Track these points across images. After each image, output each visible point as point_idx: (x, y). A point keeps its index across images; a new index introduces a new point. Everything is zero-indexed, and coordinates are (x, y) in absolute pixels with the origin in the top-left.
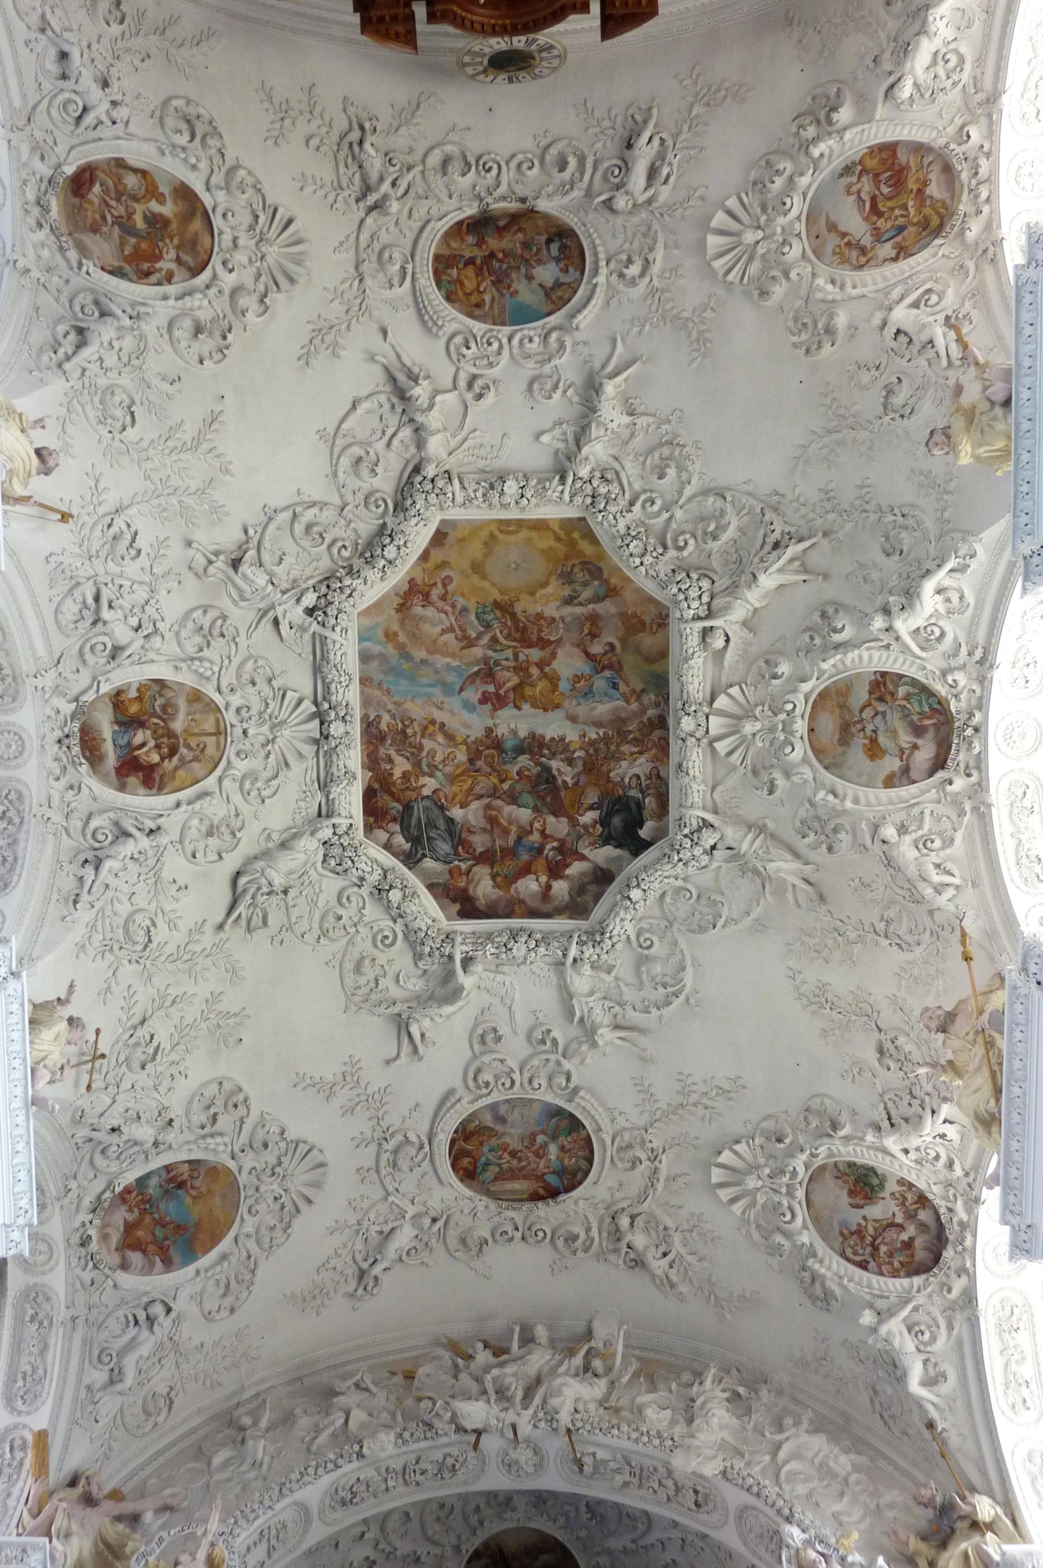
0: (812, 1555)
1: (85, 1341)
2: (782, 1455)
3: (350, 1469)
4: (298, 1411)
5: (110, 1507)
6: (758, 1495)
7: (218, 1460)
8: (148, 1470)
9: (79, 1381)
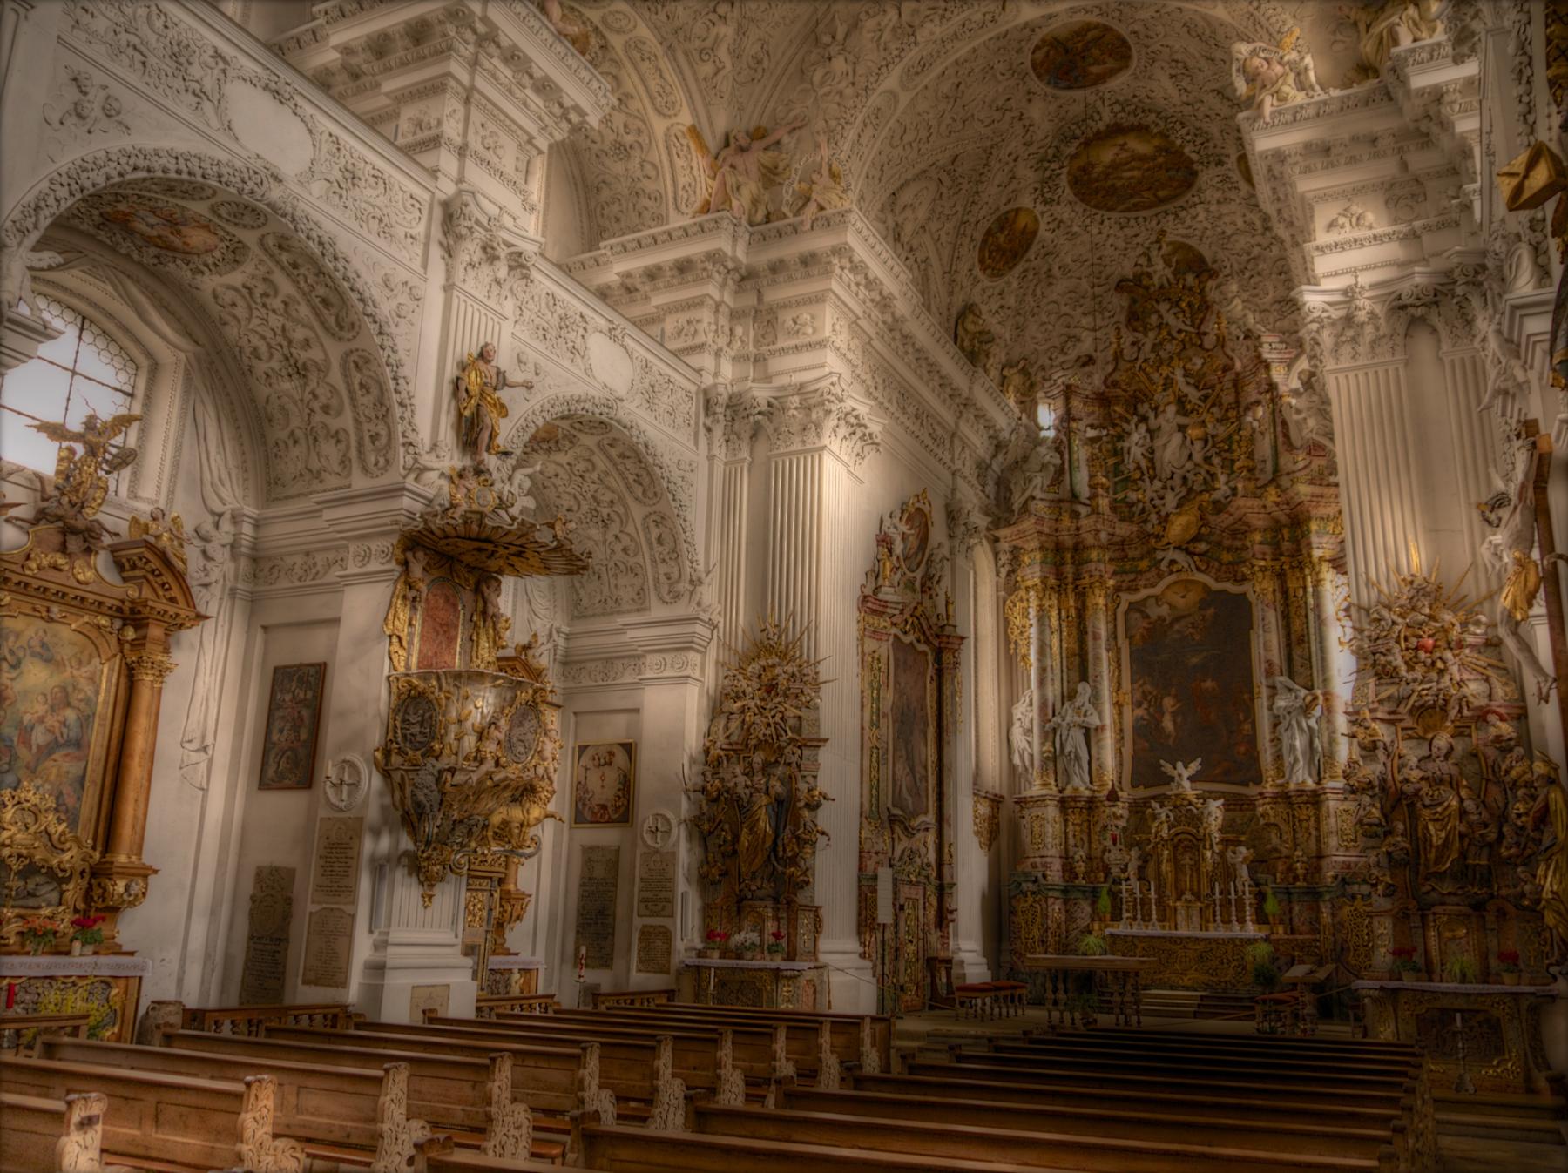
0: (1256, 62)
1: (686, 53)
3: (912, 55)
4: (863, 16)
5: (757, 145)
7: (817, 78)
8: (773, 100)
9: (697, 80)
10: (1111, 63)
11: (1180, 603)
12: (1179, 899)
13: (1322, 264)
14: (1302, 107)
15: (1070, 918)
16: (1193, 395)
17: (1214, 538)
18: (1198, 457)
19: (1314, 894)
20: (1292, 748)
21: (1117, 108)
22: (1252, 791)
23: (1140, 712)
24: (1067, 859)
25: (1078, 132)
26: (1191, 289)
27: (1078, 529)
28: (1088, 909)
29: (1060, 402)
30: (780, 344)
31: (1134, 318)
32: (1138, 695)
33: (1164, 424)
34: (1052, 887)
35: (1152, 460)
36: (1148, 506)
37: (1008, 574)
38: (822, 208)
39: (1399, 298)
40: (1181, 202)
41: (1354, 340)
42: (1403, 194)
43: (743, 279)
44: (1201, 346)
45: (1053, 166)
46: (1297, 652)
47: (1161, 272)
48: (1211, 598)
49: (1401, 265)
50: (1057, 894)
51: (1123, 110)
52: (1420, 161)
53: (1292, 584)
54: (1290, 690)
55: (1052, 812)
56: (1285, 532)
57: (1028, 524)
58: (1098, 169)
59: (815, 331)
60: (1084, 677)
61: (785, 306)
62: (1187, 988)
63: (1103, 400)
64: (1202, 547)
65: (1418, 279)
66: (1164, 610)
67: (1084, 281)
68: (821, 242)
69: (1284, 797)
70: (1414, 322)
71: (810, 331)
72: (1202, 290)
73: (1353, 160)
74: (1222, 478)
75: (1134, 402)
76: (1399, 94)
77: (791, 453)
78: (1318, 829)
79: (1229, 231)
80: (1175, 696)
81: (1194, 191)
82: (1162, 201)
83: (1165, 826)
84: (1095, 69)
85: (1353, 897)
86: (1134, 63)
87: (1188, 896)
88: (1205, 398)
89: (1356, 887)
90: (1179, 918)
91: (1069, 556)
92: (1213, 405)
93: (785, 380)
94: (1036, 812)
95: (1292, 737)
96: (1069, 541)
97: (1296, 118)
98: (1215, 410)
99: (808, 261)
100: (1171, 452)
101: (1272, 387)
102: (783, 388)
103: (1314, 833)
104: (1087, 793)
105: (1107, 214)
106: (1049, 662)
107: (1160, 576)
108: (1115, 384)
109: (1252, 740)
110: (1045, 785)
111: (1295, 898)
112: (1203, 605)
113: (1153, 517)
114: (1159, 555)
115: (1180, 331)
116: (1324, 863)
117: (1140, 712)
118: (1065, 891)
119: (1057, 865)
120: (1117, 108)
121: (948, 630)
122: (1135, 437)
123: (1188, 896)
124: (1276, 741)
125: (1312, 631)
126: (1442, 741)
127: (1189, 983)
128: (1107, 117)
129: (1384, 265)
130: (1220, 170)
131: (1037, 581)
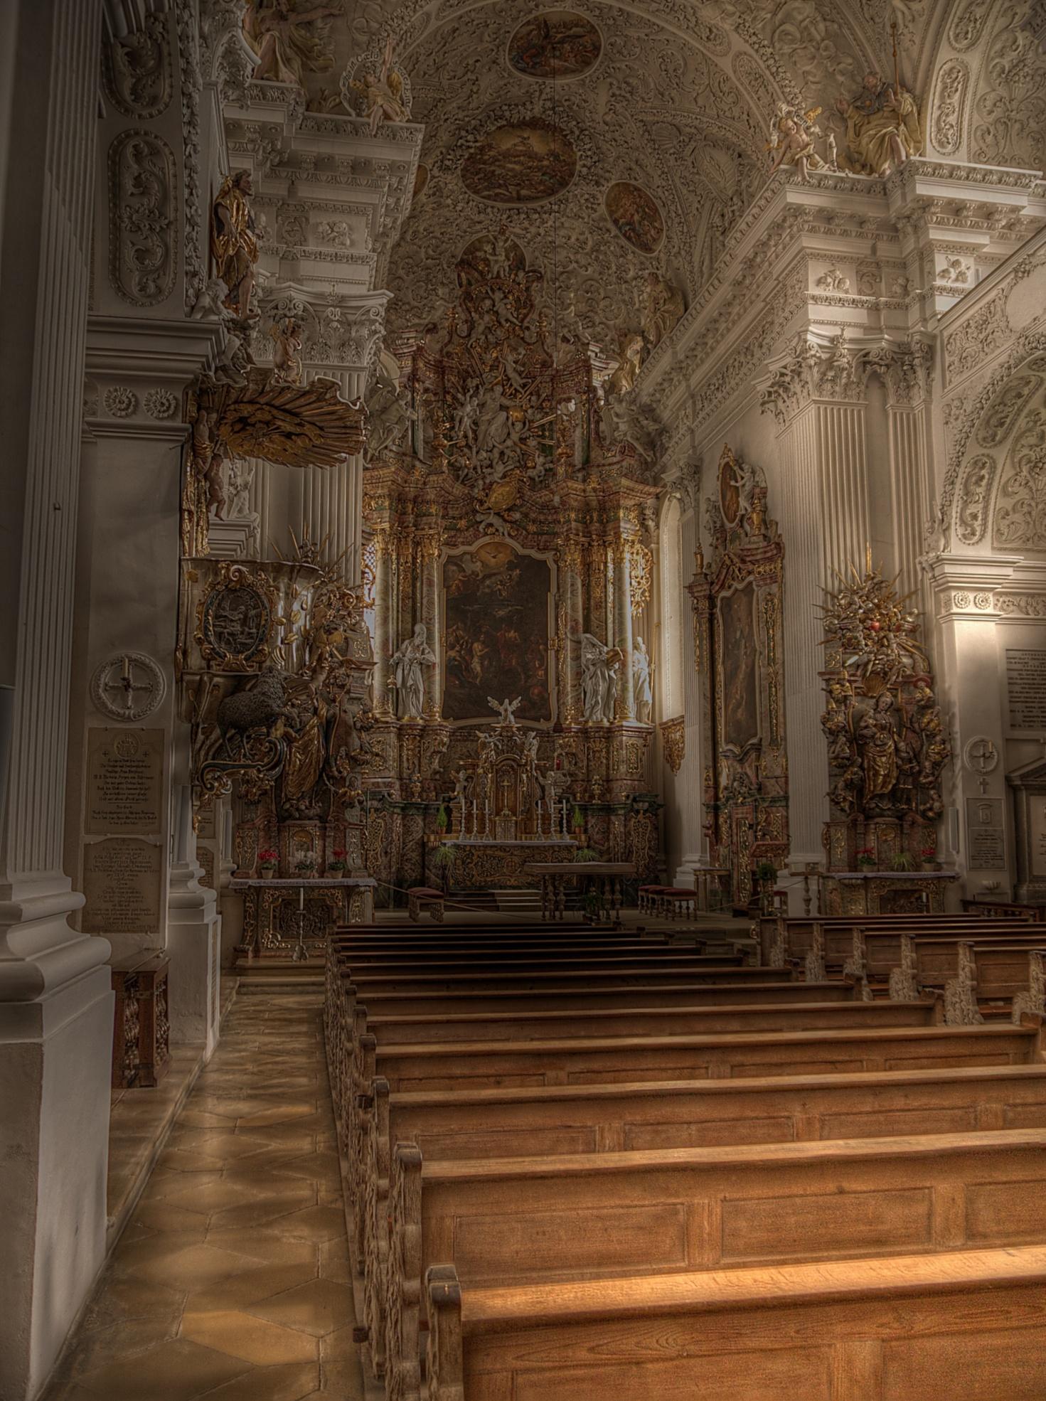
0: (790, 123)
2: (780, 16)
6: (757, 51)
10: (571, 63)
12: (498, 814)
13: (814, 311)
14: (826, 176)
15: (407, 831)
16: (517, 381)
17: (524, 509)
18: (515, 437)
19: (608, 810)
20: (595, 692)
21: (549, 104)
23: (452, 654)
25: (507, 114)
28: (421, 823)
29: (409, 362)
30: (311, 248)
32: (452, 639)
33: (489, 401)
36: (472, 474)
38: (387, 117)
39: (866, 355)
41: (833, 380)
42: (868, 272)
43: (280, 164)
45: (470, 137)
47: (500, 263)
48: (520, 562)
49: (867, 329)
51: (553, 109)
52: (886, 250)
54: (594, 645)
58: (492, 153)
59: (353, 244)
61: (319, 207)
62: (514, 888)
64: (517, 516)
65: (884, 344)
68: (382, 153)
69: (584, 733)
70: (875, 376)
71: (348, 242)
72: (527, 289)
73: (845, 233)
75: (465, 376)
76: (897, 194)
77: (349, 369)
78: (607, 759)
80: (483, 643)
81: (552, 199)
82: (520, 199)
84: (555, 63)
85: (638, 812)
86: (589, 72)
88: (524, 386)
92: (531, 394)
93: (326, 288)
95: (597, 684)
96: (411, 491)
97: (819, 184)
98: (534, 398)
99: (359, 167)
101: (591, 389)
102: (321, 296)
108: (449, 355)
109: (545, 684)
112: (511, 566)
113: (481, 482)
115: (507, 320)
116: (615, 785)
117: (452, 654)
118: (403, 809)
120: (549, 104)
122: (468, 408)
126: (888, 698)
127: (515, 883)
128: (537, 110)
129: (856, 326)
130: (592, 189)
131: (386, 526)
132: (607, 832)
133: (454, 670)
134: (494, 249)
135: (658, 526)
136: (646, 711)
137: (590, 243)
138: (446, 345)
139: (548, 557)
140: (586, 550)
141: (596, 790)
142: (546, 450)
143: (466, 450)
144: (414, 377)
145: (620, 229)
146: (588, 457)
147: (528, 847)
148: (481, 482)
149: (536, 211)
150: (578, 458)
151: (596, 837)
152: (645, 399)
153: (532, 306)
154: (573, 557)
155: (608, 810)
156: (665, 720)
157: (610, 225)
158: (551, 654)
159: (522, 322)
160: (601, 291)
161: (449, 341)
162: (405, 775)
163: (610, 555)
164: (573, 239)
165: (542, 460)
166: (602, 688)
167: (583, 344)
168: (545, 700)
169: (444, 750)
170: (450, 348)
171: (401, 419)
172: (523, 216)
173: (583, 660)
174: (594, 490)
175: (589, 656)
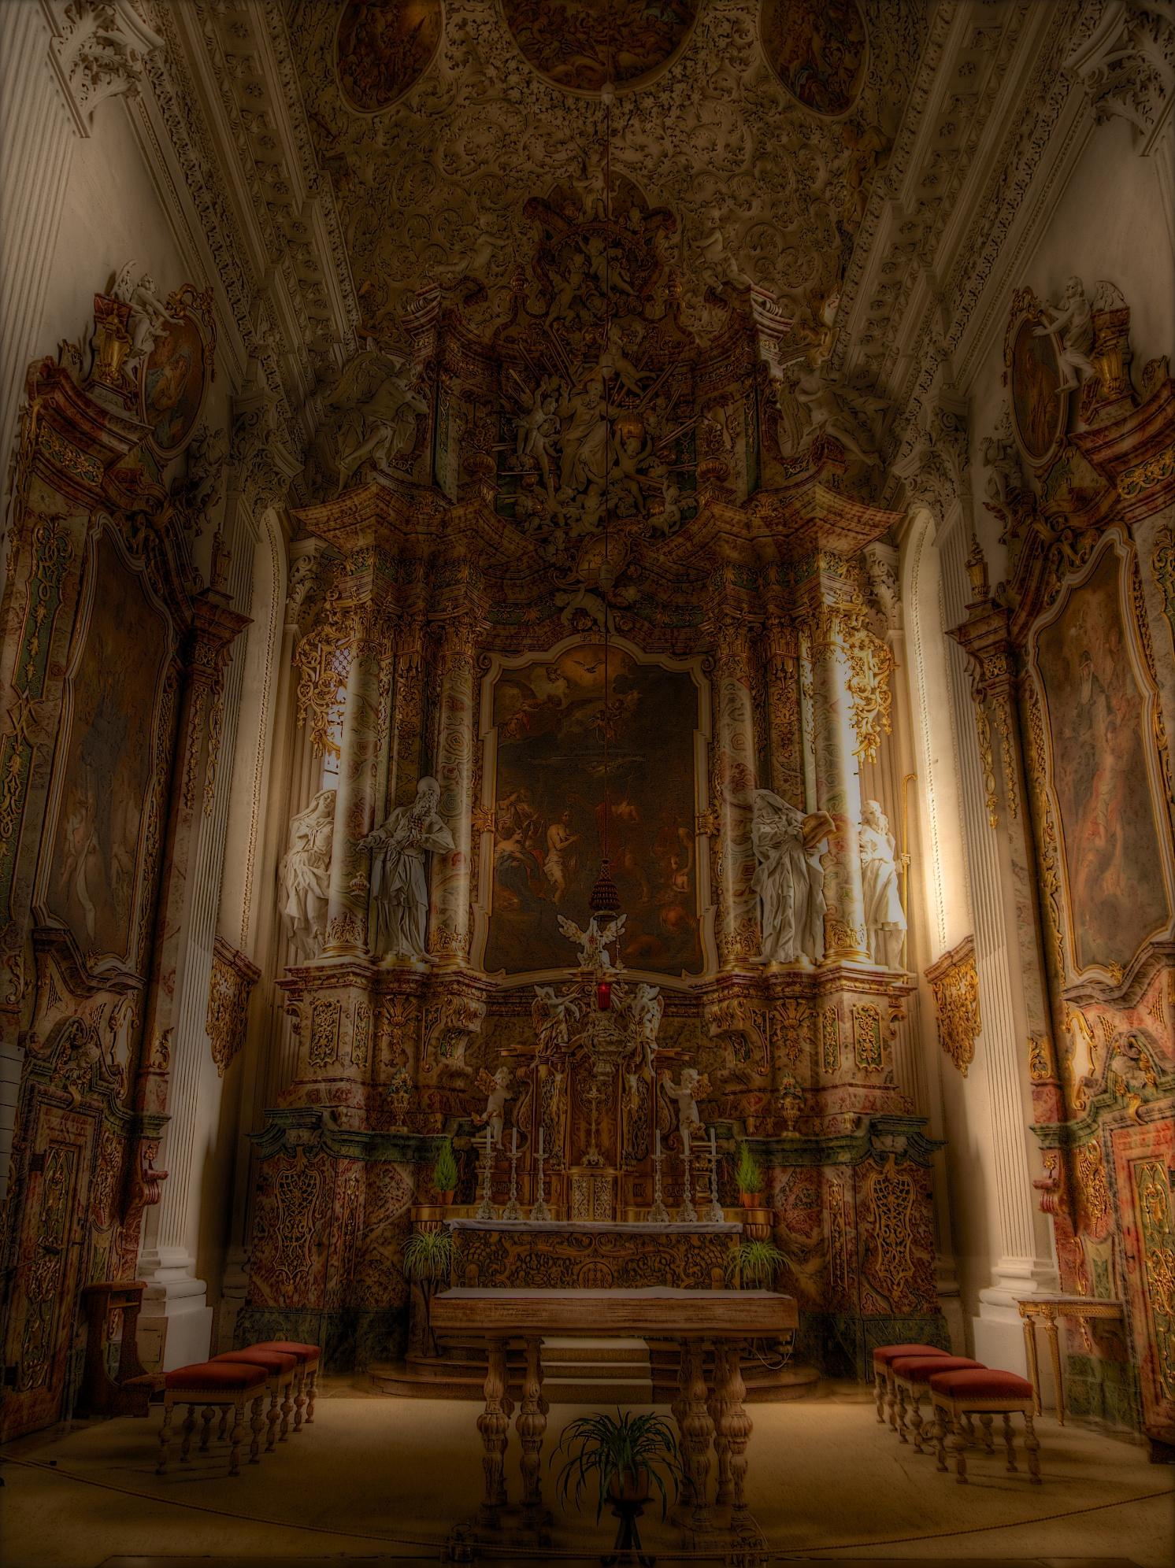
11: (588, 678)
12: (576, 1161)
15: (376, 1197)
18: (628, 465)
19: (816, 1152)
20: (781, 902)
22: (685, 982)
23: (508, 846)
24: (372, 1083)
26: (635, 233)
27: (444, 524)
28: (408, 1181)
31: (546, 256)
32: (507, 818)
33: (581, 409)
34: (346, 1137)
35: (556, 462)
37: (309, 599)
40: (648, 85)
44: (641, 315)
46: (779, 758)
47: (594, 193)
50: (355, 1151)
53: (778, 649)
54: (777, 810)
55: (354, 997)
56: (772, 575)
57: (362, 499)
60: (426, 768)
63: (493, 359)
64: (631, 593)
66: (559, 688)
67: (474, 198)
69: (762, 988)
72: (648, 242)
74: (670, 494)
75: (537, 371)
78: (813, 1042)
79: (697, 166)
83: (563, 1027)
85: (883, 1157)
87: (593, 1155)
89: (888, 1141)
90: (576, 1196)
91: (421, 572)
92: (657, 395)
94: (326, 996)
96: (425, 549)
98: (660, 401)
100: (589, 448)
103: (807, 1047)
104: (421, 967)
105: (536, 73)
106: (371, 737)
107: (557, 636)
108: (511, 340)
109: (688, 901)
110: (346, 947)
111: (777, 1159)
113: (559, 534)
114: (560, 600)
115: (614, 288)
116: (832, 1098)
117: (508, 846)
118: (370, 1147)
119: (358, 1095)
121: (213, 598)
122: (539, 416)
123: (593, 1155)
124: (748, 891)
125: (809, 726)
131: (366, 597)
132: (815, 1204)
133: (518, 877)
134: (584, 169)
135: (898, 597)
136: (895, 947)
137: (749, 146)
138: (505, 326)
139: (694, 665)
140: (758, 641)
141: (790, 1108)
142: (685, 481)
143: (537, 489)
144: (437, 365)
145: (791, 86)
146: (758, 478)
147: (633, 1237)
148: (559, 534)
149: (649, 94)
150: (741, 486)
151: (794, 1215)
152: (857, 355)
153: (656, 264)
154: (735, 649)
155: (816, 1152)
156: (935, 958)
157: (776, 88)
158: (702, 843)
159: (640, 290)
160: (778, 240)
161: (512, 322)
162: (383, 1077)
163: (805, 646)
164: (720, 147)
165: (670, 494)
166: (795, 893)
167: (741, 292)
168: (688, 929)
169: (475, 1026)
170: (513, 331)
171: (398, 416)
172: (628, 107)
173: (755, 836)
174: (768, 522)
175: (767, 829)
